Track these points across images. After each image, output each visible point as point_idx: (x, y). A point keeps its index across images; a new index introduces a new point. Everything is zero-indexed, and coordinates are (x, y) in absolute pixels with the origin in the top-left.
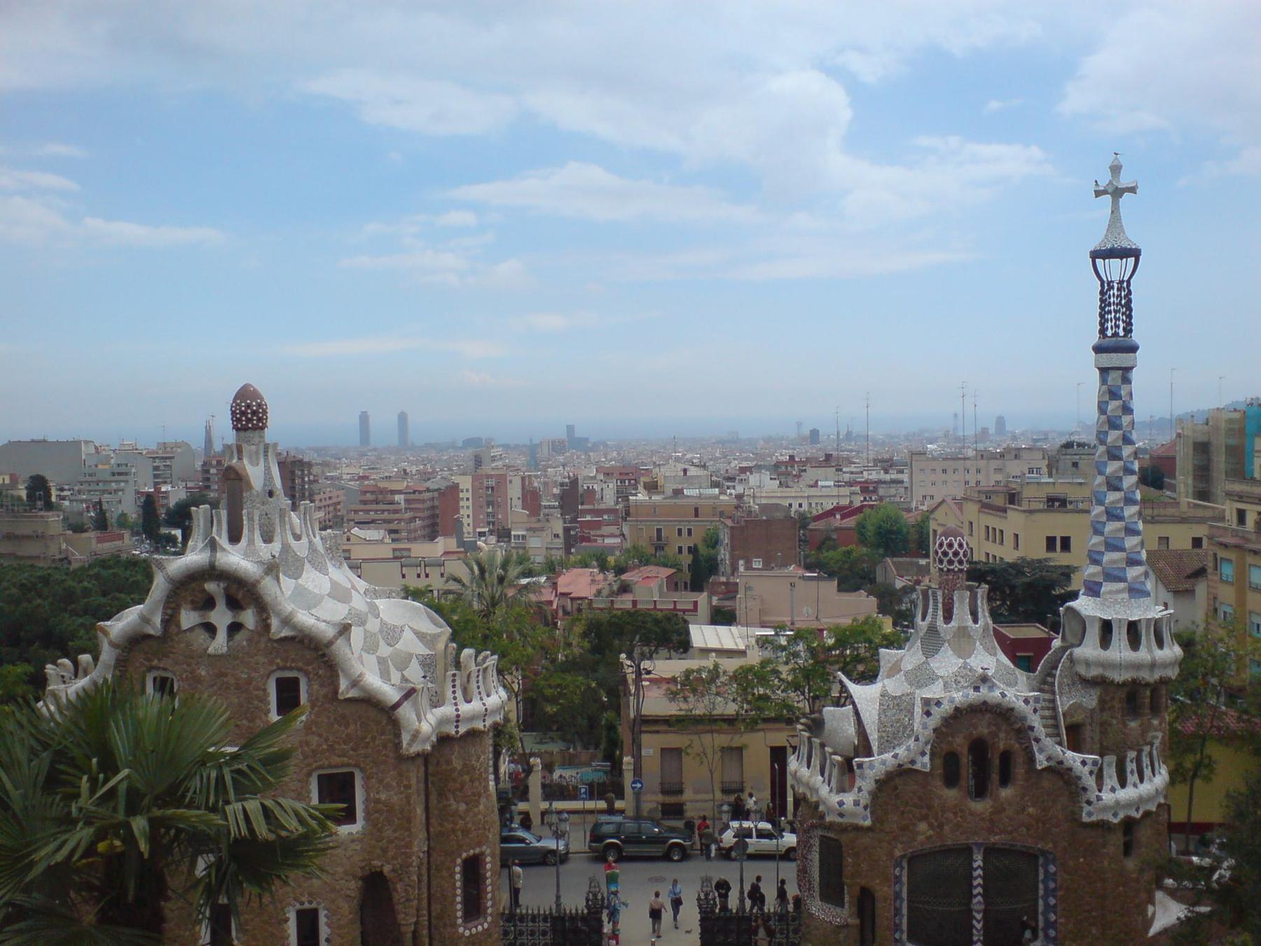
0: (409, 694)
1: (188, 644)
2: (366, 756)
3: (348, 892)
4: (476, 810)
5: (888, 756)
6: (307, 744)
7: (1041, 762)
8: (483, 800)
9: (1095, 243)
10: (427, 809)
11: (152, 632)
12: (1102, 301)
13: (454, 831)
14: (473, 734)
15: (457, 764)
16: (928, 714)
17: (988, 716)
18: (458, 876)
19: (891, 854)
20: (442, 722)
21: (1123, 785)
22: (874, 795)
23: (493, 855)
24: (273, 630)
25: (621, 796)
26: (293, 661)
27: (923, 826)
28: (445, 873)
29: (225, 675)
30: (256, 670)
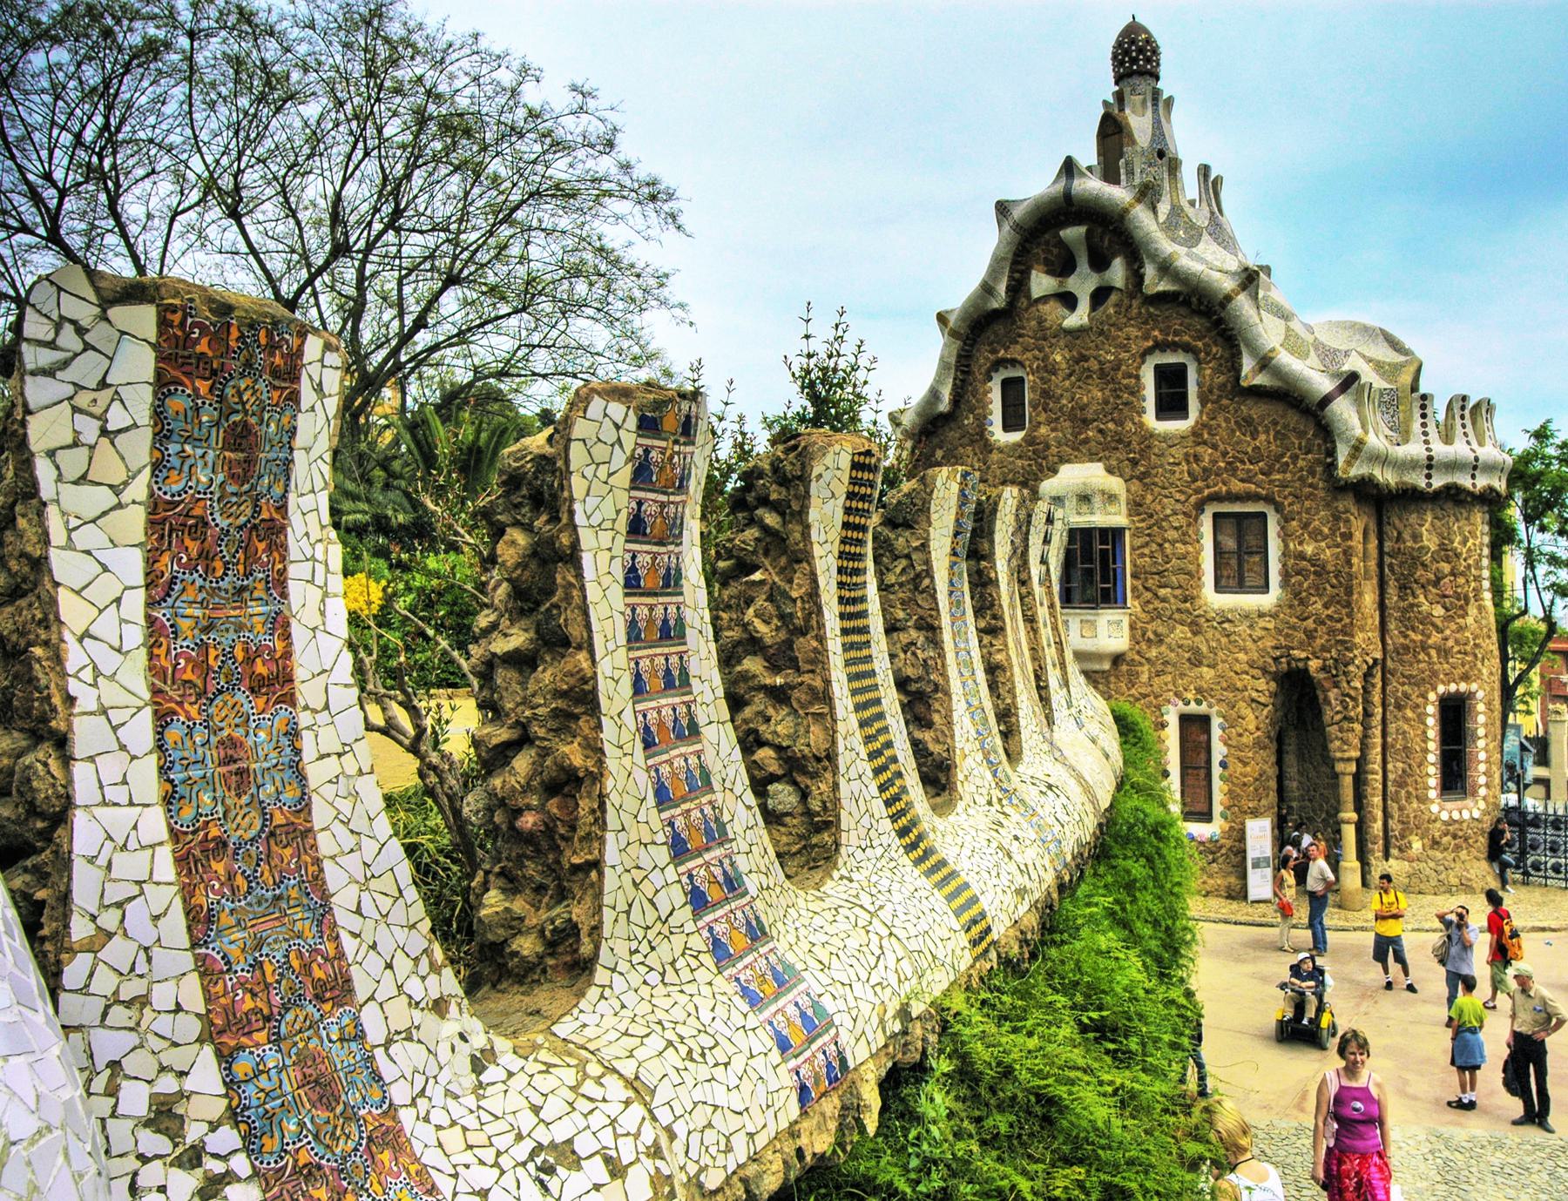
1: (1041, 321)
2: (1284, 485)
3: (1254, 695)
4: (1460, 621)
6: (1197, 458)
8: (1472, 610)
10: (1382, 606)
13: (1424, 647)
14: (1453, 496)
15: (1430, 542)
18: (1431, 721)
23: (1489, 704)
24: (1147, 281)
26: (1176, 333)
28: (1409, 713)
29: (1085, 358)
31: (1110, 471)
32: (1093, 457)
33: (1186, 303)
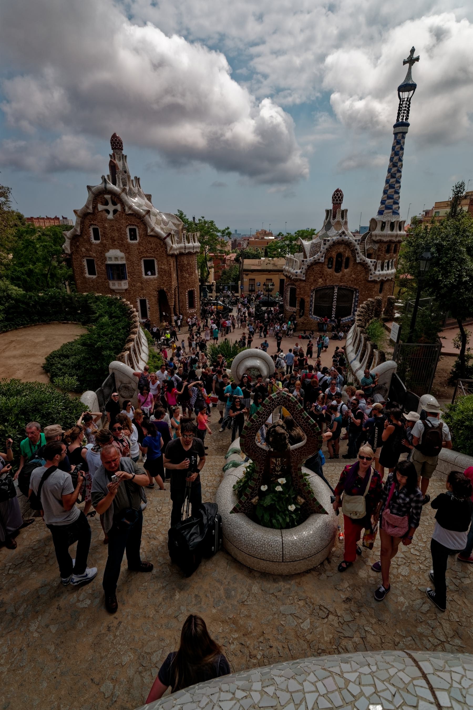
0: (169, 234)
2: (157, 254)
5: (312, 258)
7: (358, 260)
9: (401, 81)
10: (177, 275)
11: (89, 211)
12: (399, 107)
14: (190, 254)
15: (186, 262)
16: (325, 244)
17: (343, 245)
19: (310, 289)
20: (181, 248)
21: (382, 270)
22: (307, 270)
25: (237, 292)
27: (320, 280)
29: (113, 226)
30: (122, 225)
31: (121, 251)
32: (117, 248)
33: (135, 216)
